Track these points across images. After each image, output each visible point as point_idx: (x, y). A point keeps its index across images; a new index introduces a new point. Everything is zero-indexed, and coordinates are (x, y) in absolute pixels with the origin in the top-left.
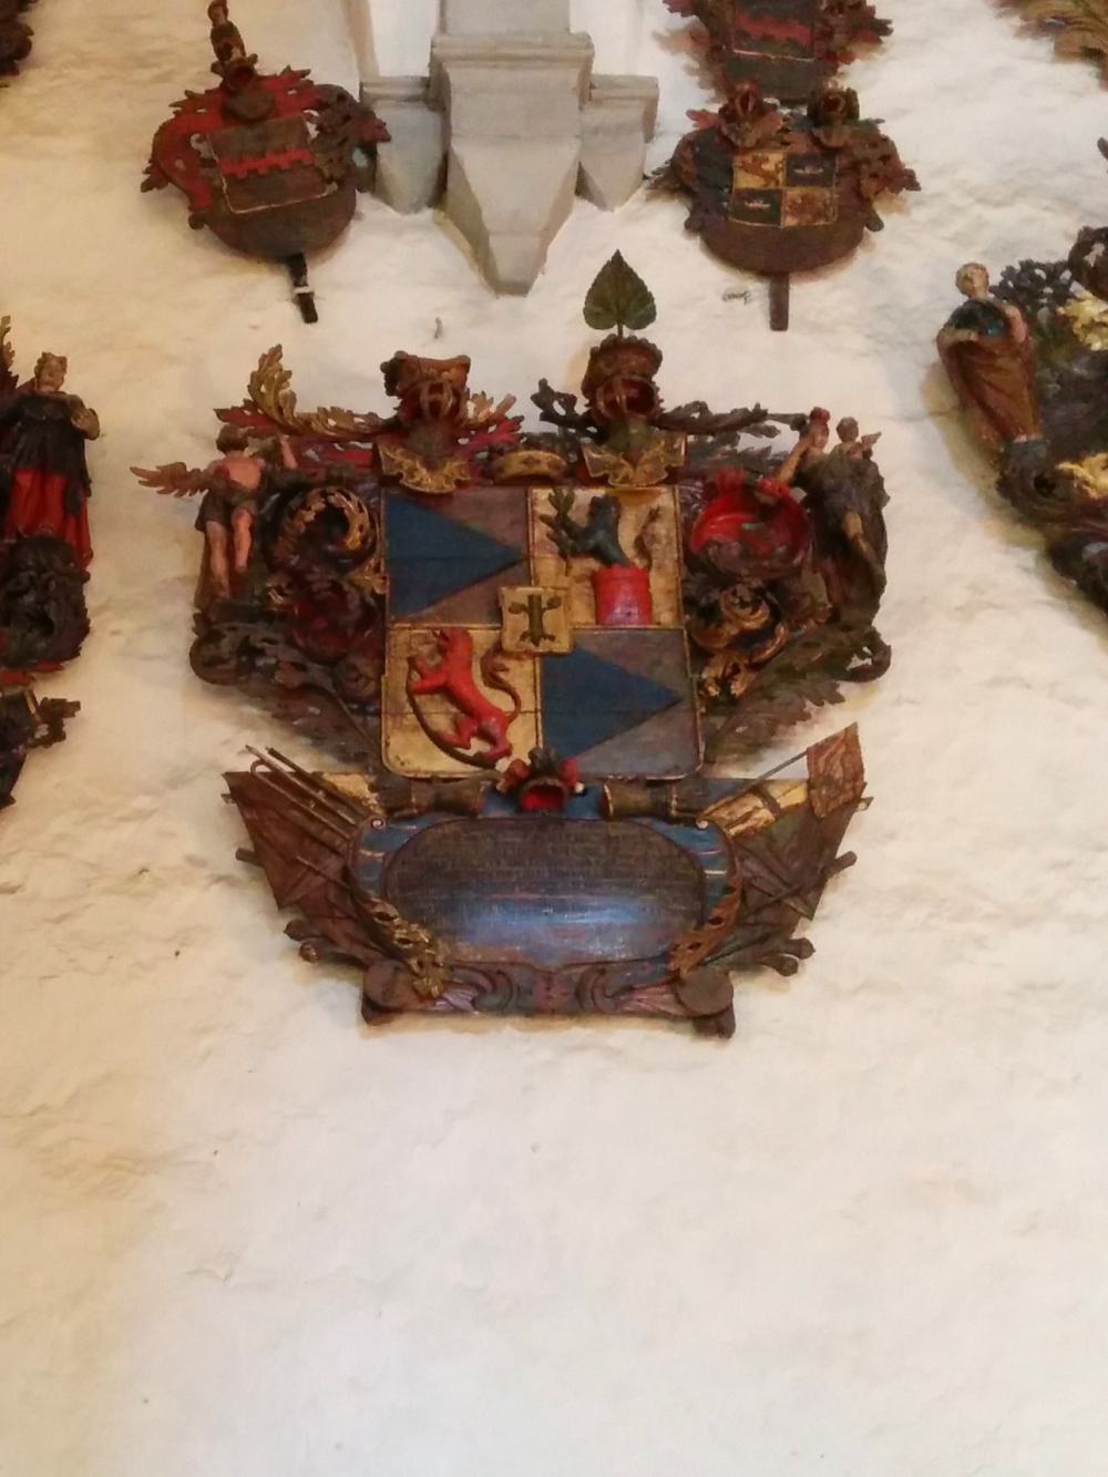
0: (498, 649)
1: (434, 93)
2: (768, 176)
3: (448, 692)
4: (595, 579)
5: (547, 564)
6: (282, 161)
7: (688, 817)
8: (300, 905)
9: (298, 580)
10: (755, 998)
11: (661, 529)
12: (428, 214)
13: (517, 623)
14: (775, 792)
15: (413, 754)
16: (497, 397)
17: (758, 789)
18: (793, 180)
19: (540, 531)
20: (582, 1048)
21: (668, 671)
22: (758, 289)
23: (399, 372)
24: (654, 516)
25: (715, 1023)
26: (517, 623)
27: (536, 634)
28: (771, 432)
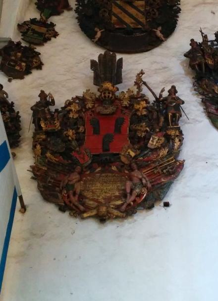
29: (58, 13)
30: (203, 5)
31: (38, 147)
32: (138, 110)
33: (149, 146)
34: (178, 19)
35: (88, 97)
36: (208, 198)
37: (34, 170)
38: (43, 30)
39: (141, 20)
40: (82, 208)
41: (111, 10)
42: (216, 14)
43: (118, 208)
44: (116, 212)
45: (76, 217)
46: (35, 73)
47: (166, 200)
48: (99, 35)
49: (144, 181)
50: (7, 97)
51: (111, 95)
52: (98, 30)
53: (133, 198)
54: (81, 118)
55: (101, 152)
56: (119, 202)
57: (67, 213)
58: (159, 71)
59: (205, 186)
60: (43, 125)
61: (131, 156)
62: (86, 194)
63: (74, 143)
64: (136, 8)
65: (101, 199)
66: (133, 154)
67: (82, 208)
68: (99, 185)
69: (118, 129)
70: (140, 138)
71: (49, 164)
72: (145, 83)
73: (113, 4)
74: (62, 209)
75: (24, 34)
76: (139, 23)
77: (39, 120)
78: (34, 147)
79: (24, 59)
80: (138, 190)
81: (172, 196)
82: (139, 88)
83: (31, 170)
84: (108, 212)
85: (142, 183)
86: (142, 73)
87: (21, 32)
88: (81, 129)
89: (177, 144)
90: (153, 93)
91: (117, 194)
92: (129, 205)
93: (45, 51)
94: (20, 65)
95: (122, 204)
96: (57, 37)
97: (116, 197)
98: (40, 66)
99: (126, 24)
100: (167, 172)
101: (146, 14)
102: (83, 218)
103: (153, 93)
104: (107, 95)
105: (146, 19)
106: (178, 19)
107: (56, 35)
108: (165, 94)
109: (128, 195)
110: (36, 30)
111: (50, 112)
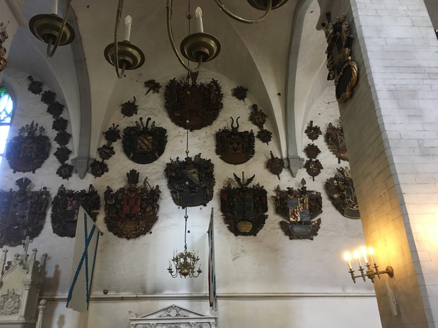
0: (297, 211)
1: (288, 159)
2: (312, 167)
3: (294, 215)
5: (299, 204)
6: (277, 166)
9: (283, 206)
10: (315, 237)
11: (307, 201)
12: (287, 169)
13: (298, 209)
14: (315, 222)
15: (292, 219)
16: (295, 189)
17: (314, 222)
18: (314, 168)
19: (299, 201)
20: (304, 241)
23: (288, 188)
24: (306, 200)
25: (312, 239)
26: (298, 209)
27: (299, 210)
28: (314, 192)
29: (115, 141)
30: (178, 137)
31: (107, 210)
32: (143, 196)
33: (146, 211)
34: (166, 146)
35: (125, 189)
36: (165, 230)
38: (108, 151)
39: (150, 147)
40: (122, 235)
41: (137, 142)
42: (183, 142)
43: (134, 234)
44: (133, 236)
45: (120, 237)
46: (105, 174)
47: (150, 231)
48: (132, 155)
49: (143, 225)
50: (94, 190)
51: (134, 189)
52: (131, 153)
53: (139, 231)
54: (123, 198)
55: (129, 212)
56: (134, 233)
57: (117, 236)
58: (155, 173)
59: (165, 225)
60: (108, 202)
61: (139, 215)
62: (123, 229)
64: (148, 140)
66: (140, 214)
67: (122, 235)
68: (128, 226)
69: (136, 204)
70: (143, 208)
74: (115, 234)
75: (100, 154)
76: (149, 148)
77: (107, 199)
78: (105, 210)
79: (101, 168)
80: (140, 229)
81: (153, 230)
82: (145, 185)
83: (104, 219)
84: (131, 236)
85: (142, 226)
86: (147, 178)
87: (99, 153)
88: (123, 203)
89: (156, 210)
90: (150, 187)
91: (134, 229)
92: (138, 233)
93: (109, 162)
94: (99, 171)
95: (135, 233)
97: (133, 230)
99: (143, 149)
100: (152, 221)
101: (153, 144)
102: (122, 238)
103: (150, 187)
104: (132, 189)
106: (166, 146)
107: (114, 153)
108: (155, 188)
109: (137, 230)
110: (106, 151)
111: (111, 194)
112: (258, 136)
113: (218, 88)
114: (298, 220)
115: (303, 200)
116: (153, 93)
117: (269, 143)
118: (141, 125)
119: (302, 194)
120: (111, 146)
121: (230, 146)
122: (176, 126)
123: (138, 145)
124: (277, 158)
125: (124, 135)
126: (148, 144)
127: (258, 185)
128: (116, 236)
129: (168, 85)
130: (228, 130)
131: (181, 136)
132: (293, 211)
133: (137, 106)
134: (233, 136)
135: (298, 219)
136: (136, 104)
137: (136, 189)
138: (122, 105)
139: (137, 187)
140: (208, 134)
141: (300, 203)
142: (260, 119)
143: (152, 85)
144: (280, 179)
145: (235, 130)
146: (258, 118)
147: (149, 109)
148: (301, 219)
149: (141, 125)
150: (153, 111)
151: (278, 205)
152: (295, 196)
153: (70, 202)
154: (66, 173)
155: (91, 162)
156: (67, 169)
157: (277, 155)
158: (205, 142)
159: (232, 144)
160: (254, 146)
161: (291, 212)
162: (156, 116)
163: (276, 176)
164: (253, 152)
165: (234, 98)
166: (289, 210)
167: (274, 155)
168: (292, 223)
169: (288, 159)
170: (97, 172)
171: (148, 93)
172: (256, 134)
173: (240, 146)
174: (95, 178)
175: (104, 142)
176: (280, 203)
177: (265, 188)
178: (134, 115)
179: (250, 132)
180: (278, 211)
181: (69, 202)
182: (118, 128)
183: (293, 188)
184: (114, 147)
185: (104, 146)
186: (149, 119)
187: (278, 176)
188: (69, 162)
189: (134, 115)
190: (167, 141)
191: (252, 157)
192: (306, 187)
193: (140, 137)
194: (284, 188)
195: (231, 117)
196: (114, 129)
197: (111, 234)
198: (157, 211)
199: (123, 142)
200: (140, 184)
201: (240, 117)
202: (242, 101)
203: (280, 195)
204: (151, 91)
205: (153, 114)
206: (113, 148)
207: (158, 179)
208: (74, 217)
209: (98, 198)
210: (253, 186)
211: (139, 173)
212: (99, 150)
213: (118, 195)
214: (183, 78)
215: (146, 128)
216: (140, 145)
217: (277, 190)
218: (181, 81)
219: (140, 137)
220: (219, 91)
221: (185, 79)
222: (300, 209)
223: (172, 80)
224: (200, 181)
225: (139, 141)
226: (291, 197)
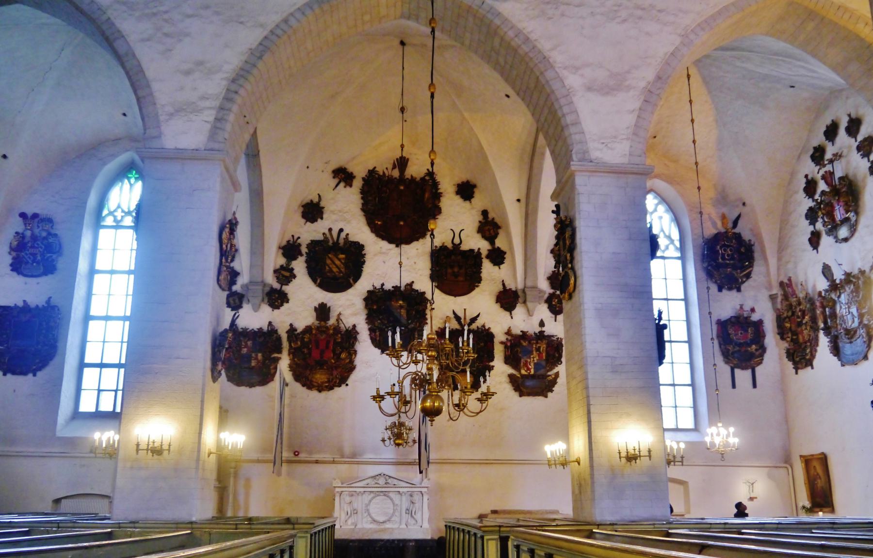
0: (530, 362)
1: (524, 291)
4: (538, 354)
5: (534, 353)
7: (545, 379)
8: (515, 387)
10: (550, 394)
11: (544, 349)
12: (523, 304)
15: (523, 372)
18: (558, 304)
19: (534, 349)
21: (544, 363)
22: (554, 316)
26: (532, 359)
27: (534, 360)
29: (295, 259)
31: (291, 355)
35: (313, 327)
37: (290, 366)
38: (287, 274)
43: (326, 387)
44: (325, 389)
48: (318, 281)
49: (337, 376)
56: (327, 384)
63: (308, 356)
64: (339, 260)
65: (319, 382)
71: (296, 364)
72: (341, 320)
73: (327, 257)
74: (303, 386)
75: (278, 278)
76: (340, 272)
78: (289, 355)
81: (349, 382)
82: (338, 323)
86: (340, 314)
87: (276, 277)
88: (310, 346)
90: (345, 326)
91: (326, 380)
92: (331, 386)
94: (278, 302)
96: (296, 279)
98: (288, 302)
101: (346, 265)
105: (345, 270)
107: (294, 277)
108: (351, 327)
112: (488, 257)
113: (435, 185)
114: (531, 373)
115: (540, 347)
116: (345, 187)
117: (502, 266)
118: (330, 239)
119: (539, 339)
120: (291, 267)
121: (450, 271)
122: (376, 238)
123: (327, 267)
124: (510, 289)
125: (307, 251)
126: (340, 265)
127: (484, 326)
128: (305, 388)
129: (366, 178)
130: (448, 248)
131: (384, 253)
132: (526, 361)
133: (323, 208)
134: (453, 257)
135: (530, 372)
136: (322, 204)
137: (327, 328)
138: (303, 206)
139: (328, 325)
140: (420, 251)
141: (536, 351)
142: (492, 231)
143: (343, 176)
144: (512, 318)
145: (456, 247)
146: (489, 230)
147: (340, 211)
148: (535, 371)
149: (330, 239)
150: (345, 215)
151: (507, 353)
152: (530, 343)
153: (244, 343)
154: (235, 303)
155: (267, 289)
156: (236, 297)
157: (510, 285)
158: (415, 263)
159: (452, 267)
160: (481, 270)
161: (523, 363)
162: (349, 222)
163: (508, 313)
164: (479, 280)
165: (458, 197)
166: (520, 360)
167: (506, 284)
168: (523, 376)
169: (524, 291)
170: (274, 303)
171: (338, 188)
172: (484, 253)
173: (463, 271)
174: (273, 310)
175: (282, 261)
176: (509, 351)
177: (492, 330)
178: (319, 220)
179: (476, 251)
180: (508, 361)
181: (243, 344)
182: (299, 241)
183: (528, 332)
184: (294, 268)
185: (282, 266)
186: (341, 230)
187: (511, 314)
188: (235, 288)
189: (319, 220)
190: (365, 262)
191: (477, 286)
192: (544, 331)
193: (330, 255)
194: (517, 331)
195: (451, 230)
196: (295, 242)
197: (298, 385)
198: (354, 358)
199: (306, 262)
200: (332, 321)
201: (463, 230)
202: (468, 202)
203: (510, 341)
204: (342, 184)
205: (345, 220)
206: (293, 269)
207: (355, 314)
208: (251, 362)
209: (279, 339)
210: (478, 327)
211: (329, 308)
212: (275, 271)
213: (304, 336)
214: (387, 168)
215: (336, 243)
216: (329, 267)
217: (508, 332)
218: (384, 173)
219: (330, 255)
220: (437, 189)
221: (390, 171)
222: (535, 359)
223: (371, 170)
224: (408, 319)
225: (328, 262)
226: (524, 344)
